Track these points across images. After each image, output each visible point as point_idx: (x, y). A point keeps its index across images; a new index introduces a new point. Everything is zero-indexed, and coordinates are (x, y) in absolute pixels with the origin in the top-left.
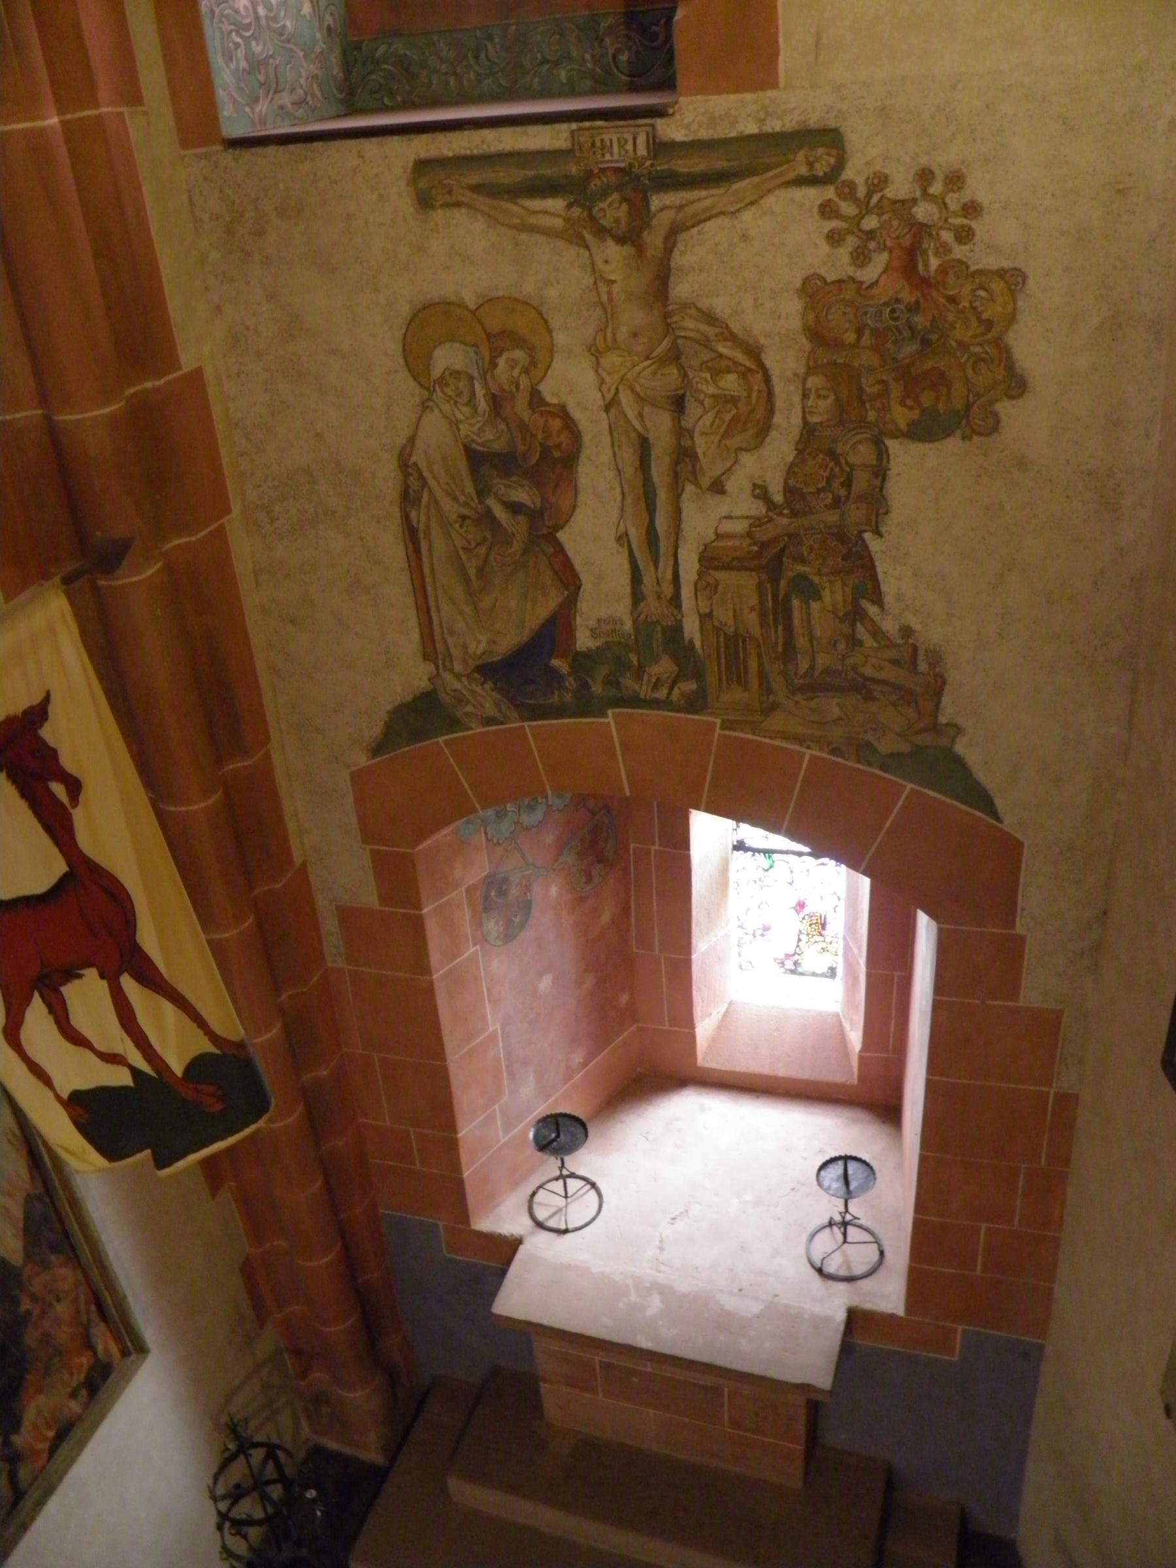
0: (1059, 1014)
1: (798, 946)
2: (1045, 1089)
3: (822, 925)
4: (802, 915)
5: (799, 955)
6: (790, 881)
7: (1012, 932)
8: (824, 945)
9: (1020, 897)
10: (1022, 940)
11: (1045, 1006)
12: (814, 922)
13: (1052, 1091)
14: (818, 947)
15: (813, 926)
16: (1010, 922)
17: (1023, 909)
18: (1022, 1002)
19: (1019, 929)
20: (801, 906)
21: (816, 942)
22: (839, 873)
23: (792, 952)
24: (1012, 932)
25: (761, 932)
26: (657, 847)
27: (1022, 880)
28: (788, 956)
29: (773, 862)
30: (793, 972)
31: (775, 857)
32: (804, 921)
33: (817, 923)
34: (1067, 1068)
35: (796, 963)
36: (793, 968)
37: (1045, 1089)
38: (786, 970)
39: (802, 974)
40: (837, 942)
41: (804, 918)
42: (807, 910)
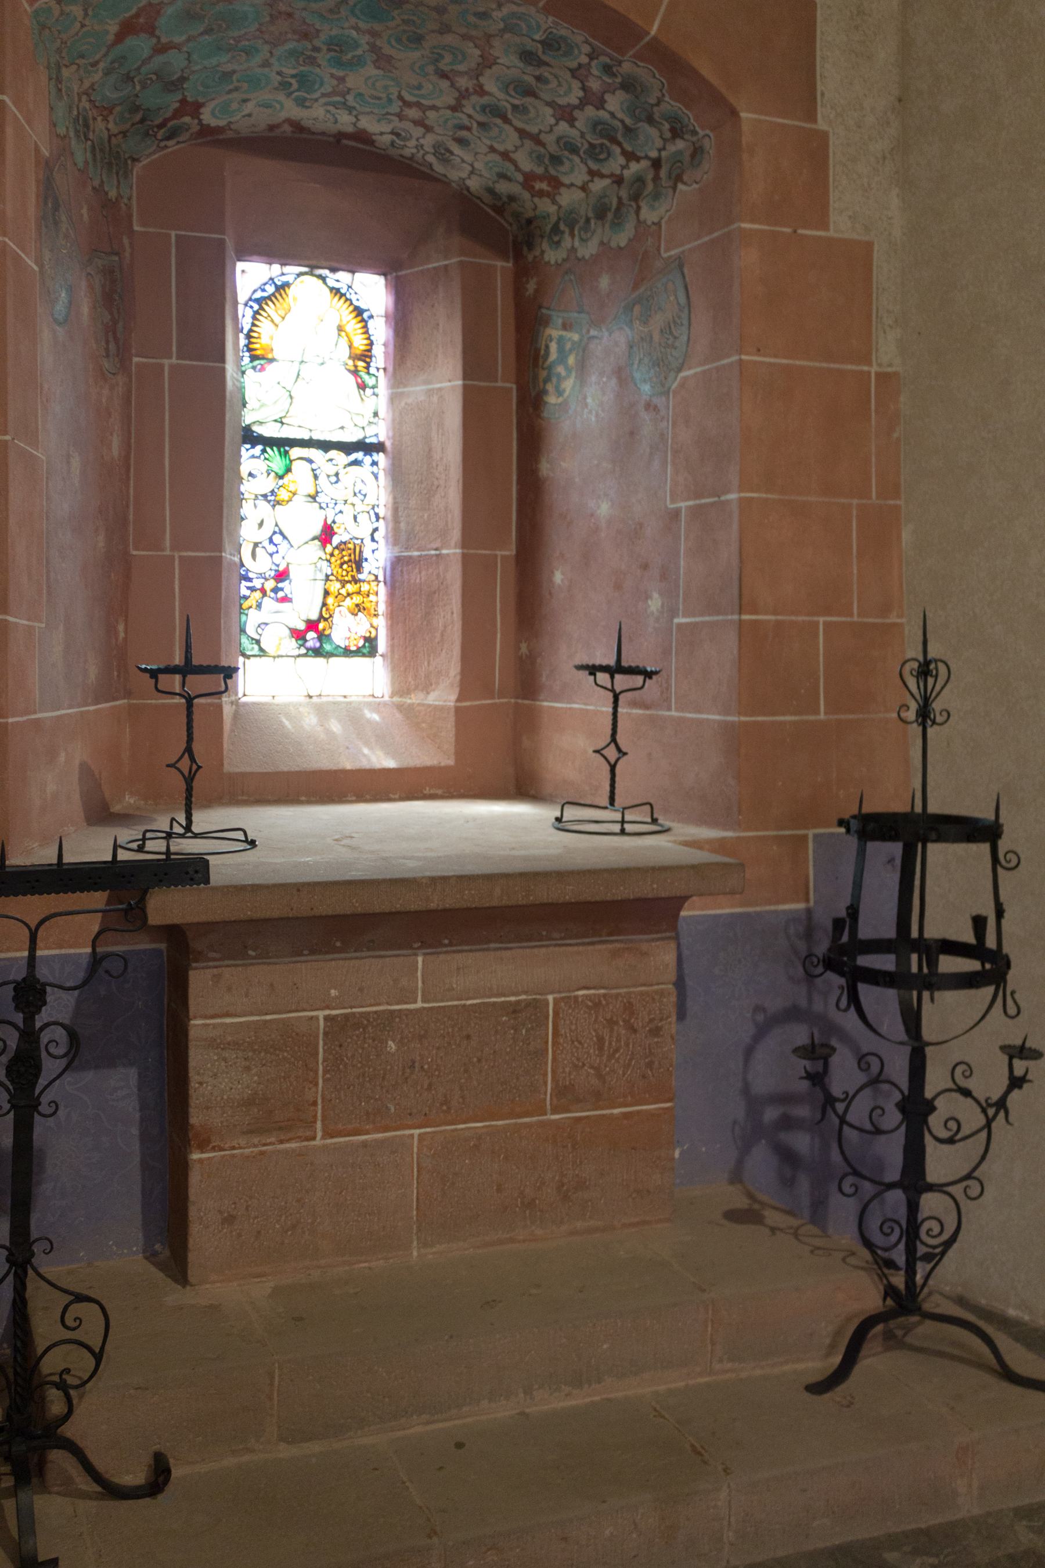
0: (869, 246)
1: (324, 604)
2: (866, 368)
3: (358, 564)
4: (329, 548)
5: (326, 620)
6: (313, 493)
7: (813, 126)
8: (357, 599)
9: (818, 77)
10: (824, 137)
11: (854, 236)
12: (346, 559)
13: (873, 371)
14: (349, 602)
15: (345, 566)
16: (811, 115)
17: (823, 94)
18: (831, 233)
19: (822, 125)
20: (327, 534)
21: (349, 595)
22: (376, 476)
23: (314, 616)
24: (813, 126)
25: (270, 585)
26: (174, 361)
27: (818, 53)
28: (312, 625)
29: (291, 461)
30: (317, 652)
31: (295, 452)
32: (333, 559)
33: (350, 561)
34: (885, 332)
35: (322, 636)
36: (318, 645)
37: (866, 368)
38: (308, 649)
39: (329, 655)
40: (377, 594)
41: (332, 555)
42: (336, 540)
